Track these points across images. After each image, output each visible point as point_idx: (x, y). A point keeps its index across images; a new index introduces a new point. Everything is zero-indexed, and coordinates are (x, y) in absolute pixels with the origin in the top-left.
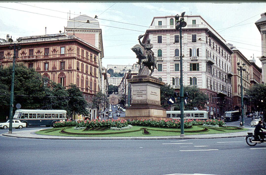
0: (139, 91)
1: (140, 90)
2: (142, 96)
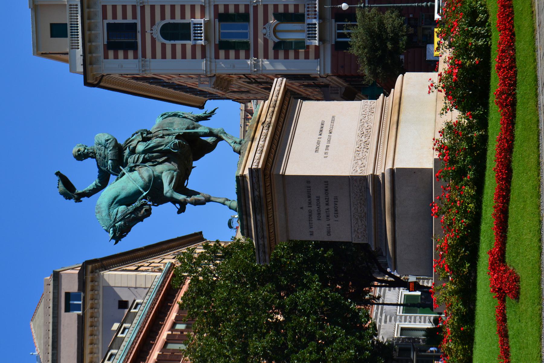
0: (310, 212)
2: (336, 198)
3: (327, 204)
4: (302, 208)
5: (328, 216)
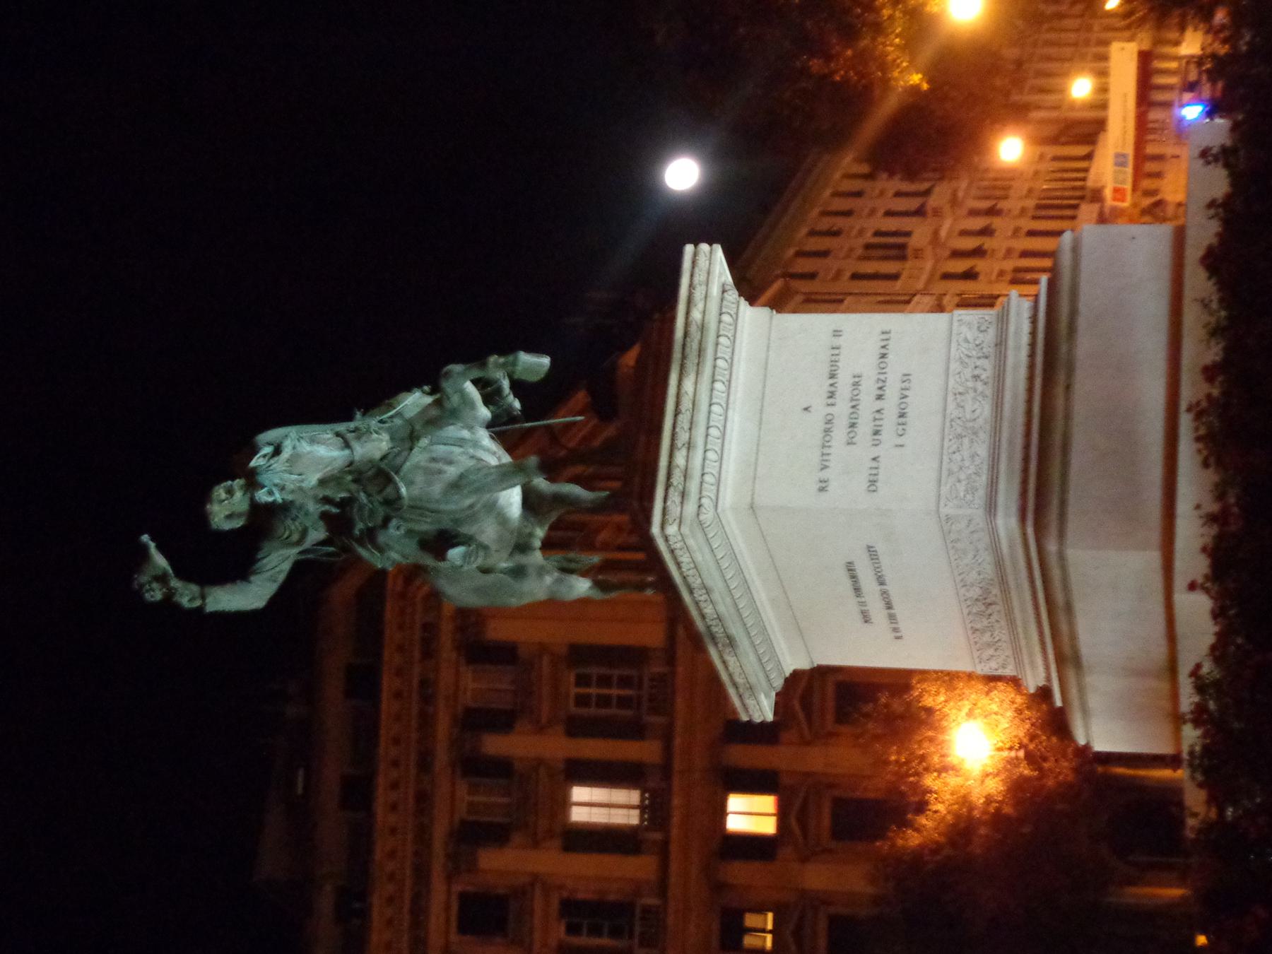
1: (820, 410)
2: (906, 377)
3: (879, 397)
4: (806, 409)
5: (876, 433)
